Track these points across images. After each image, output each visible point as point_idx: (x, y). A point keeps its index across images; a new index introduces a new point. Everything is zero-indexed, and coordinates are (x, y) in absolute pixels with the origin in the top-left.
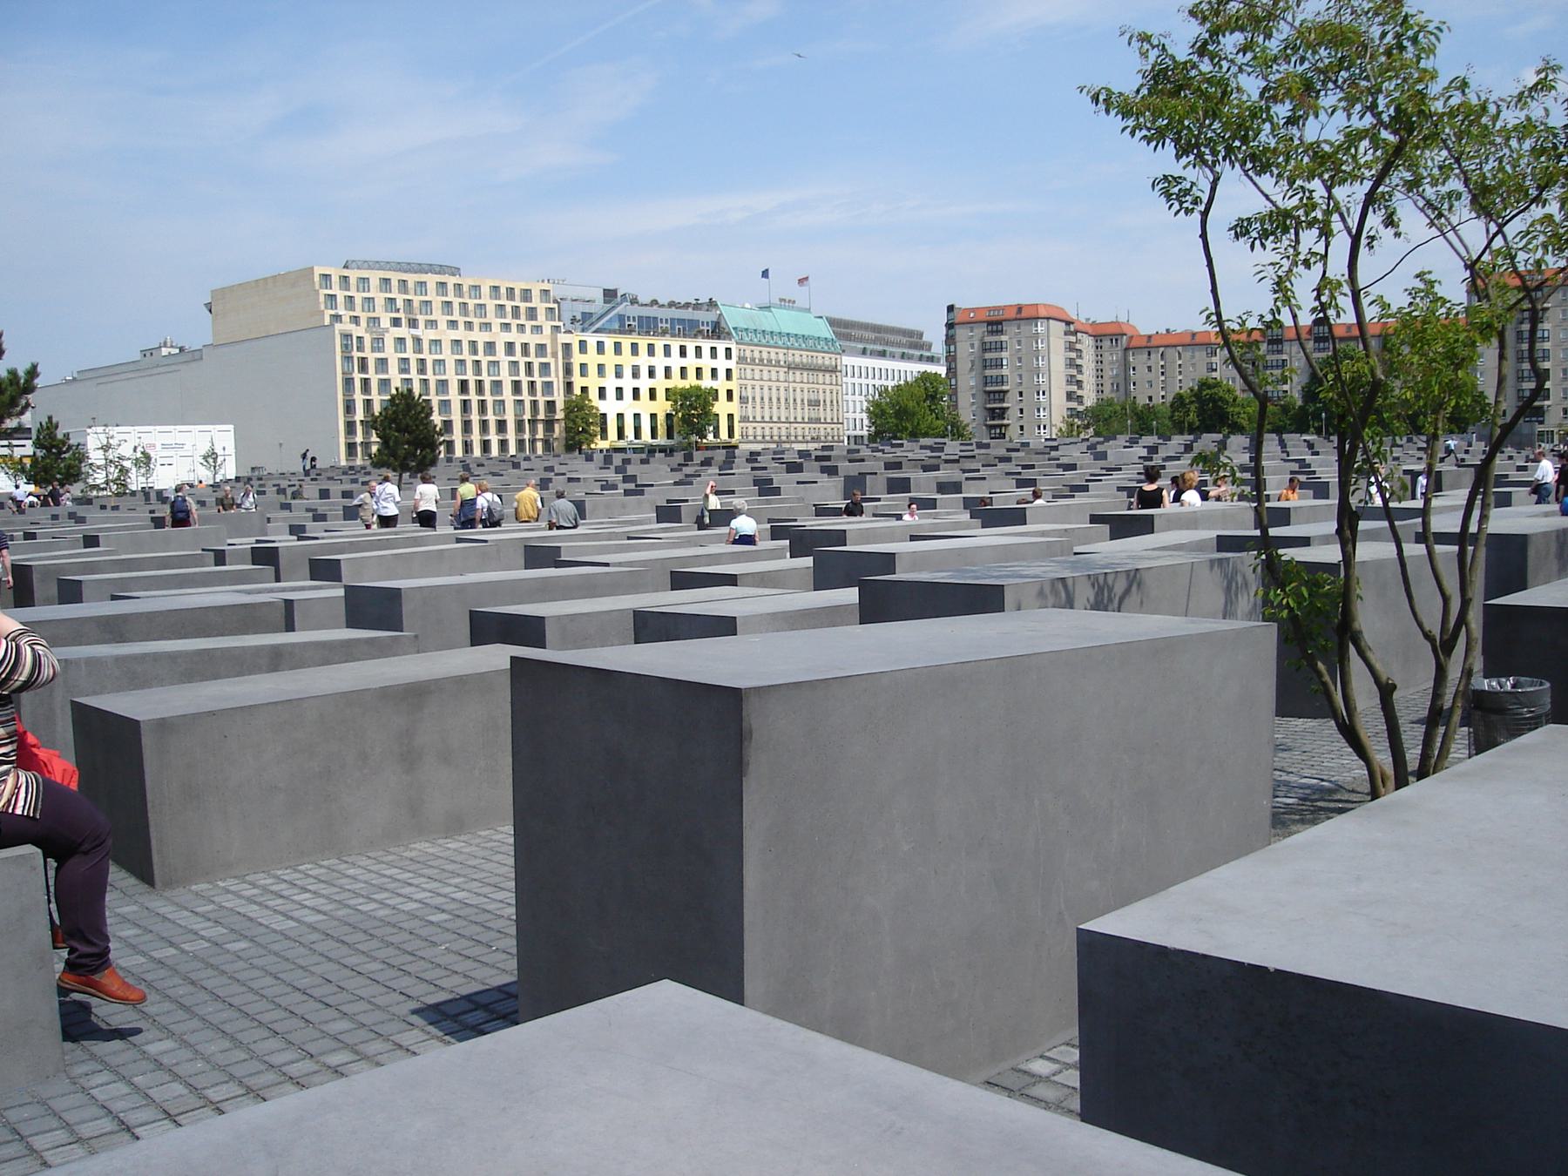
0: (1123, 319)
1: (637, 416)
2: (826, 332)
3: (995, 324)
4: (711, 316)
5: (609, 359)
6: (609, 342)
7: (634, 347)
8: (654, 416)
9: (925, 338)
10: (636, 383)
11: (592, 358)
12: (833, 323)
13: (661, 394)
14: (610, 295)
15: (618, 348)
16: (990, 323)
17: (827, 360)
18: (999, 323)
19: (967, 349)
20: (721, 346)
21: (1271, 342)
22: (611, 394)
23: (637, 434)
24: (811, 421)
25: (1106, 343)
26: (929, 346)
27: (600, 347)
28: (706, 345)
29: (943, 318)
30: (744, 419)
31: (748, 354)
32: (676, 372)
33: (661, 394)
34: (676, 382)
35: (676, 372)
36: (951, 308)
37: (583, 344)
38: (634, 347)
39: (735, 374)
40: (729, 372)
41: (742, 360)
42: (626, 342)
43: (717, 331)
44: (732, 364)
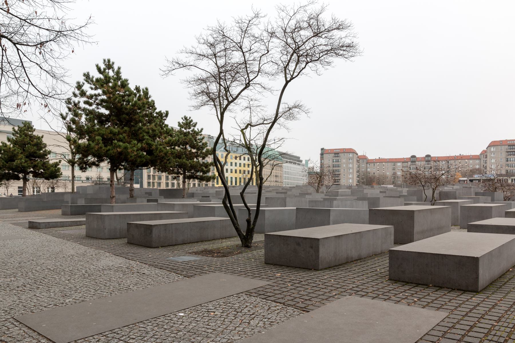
1: (232, 178)
3: (337, 153)
8: (236, 178)
9: (301, 159)
16: (335, 154)
18: (338, 154)
21: (412, 162)
23: (232, 184)
26: (301, 161)
29: (320, 152)
32: (242, 165)
33: (238, 171)
34: (242, 168)
35: (242, 165)
36: (322, 149)
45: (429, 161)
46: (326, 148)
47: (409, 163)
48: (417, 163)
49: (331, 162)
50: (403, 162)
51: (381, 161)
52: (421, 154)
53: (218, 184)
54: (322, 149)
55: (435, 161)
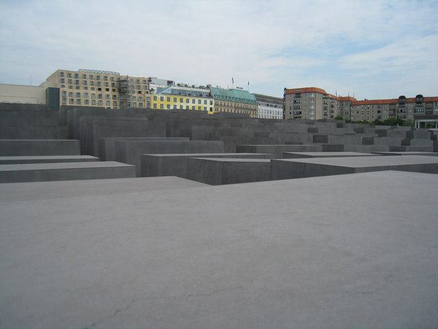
0: (351, 96)
2: (253, 98)
3: (298, 93)
4: (208, 91)
6: (165, 97)
12: (256, 96)
14: (170, 83)
15: (169, 100)
17: (253, 107)
19: (289, 103)
20: (208, 101)
21: (400, 104)
25: (344, 103)
27: (162, 99)
36: (285, 89)
37: (155, 98)
39: (213, 109)
41: (216, 105)
42: (172, 98)
43: (209, 96)
44: (212, 106)
45: (420, 103)
46: (289, 87)
47: (397, 105)
48: (406, 105)
49: (292, 102)
50: (390, 104)
51: (366, 103)
52: (410, 95)
54: (285, 89)
55: (427, 103)
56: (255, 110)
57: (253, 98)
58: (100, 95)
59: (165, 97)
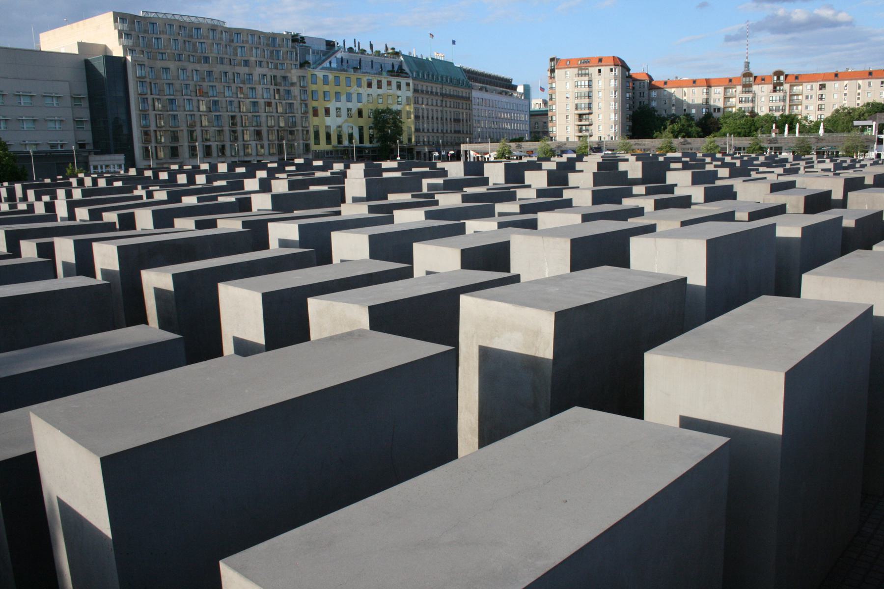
2: (462, 77)
5: (331, 88)
6: (331, 77)
7: (348, 79)
10: (350, 105)
11: (319, 87)
13: (365, 114)
17: (463, 92)
20: (403, 81)
22: (333, 112)
24: (455, 132)
27: (325, 80)
28: (394, 81)
29: (548, 65)
30: (417, 130)
31: (420, 88)
38: (348, 79)
40: (408, 98)
41: (416, 91)
42: (343, 77)
43: (398, 72)
53: (317, 142)
54: (552, 60)
56: (468, 99)
57: (462, 77)
58: (210, 73)
59: (331, 77)
